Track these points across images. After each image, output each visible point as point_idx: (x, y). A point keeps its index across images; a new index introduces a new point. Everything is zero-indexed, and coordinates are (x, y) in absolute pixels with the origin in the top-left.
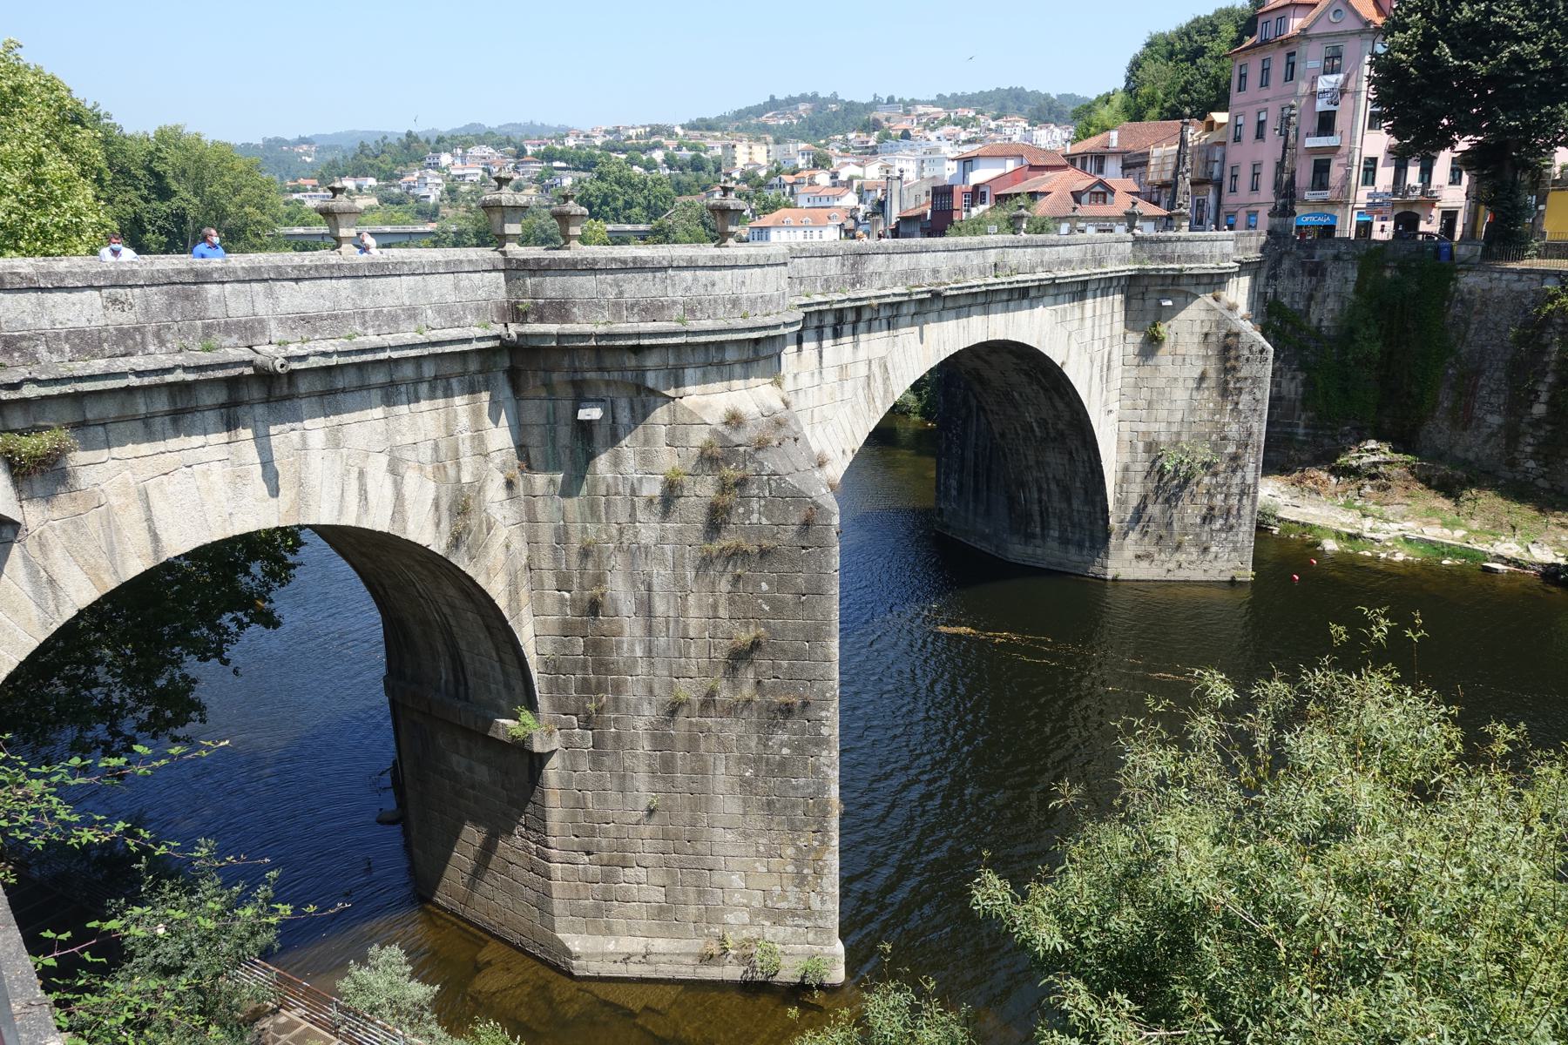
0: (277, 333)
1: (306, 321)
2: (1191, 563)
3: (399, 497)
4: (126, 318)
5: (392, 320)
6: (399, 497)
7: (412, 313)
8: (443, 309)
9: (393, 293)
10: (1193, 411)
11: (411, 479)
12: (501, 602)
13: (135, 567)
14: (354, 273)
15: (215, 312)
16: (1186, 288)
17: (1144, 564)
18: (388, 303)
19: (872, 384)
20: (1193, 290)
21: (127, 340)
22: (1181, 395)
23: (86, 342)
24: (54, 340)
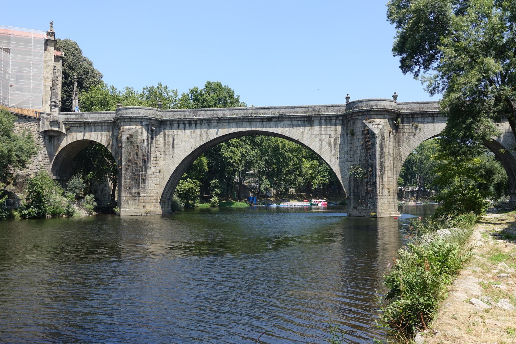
0: (89, 119)
1: (92, 118)
2: (364, 210)
3: (101, 139)
4: (76, 117)
5: (102, 118)
6: (101, 139)
7: (104, 118)
8: (108, 117)
9: (103, 115)
10: (361, 156)
11: (103, 137)
12: (114, 156)
13: (74, 140)
14: (98, 113)
15: (84, 117)
16: (355, 117)
17: (355, 211)
18: (102, 117)
19: (202, 136)
20: (357, 117)
21: (76, 119)
22: (358, 152)
23: (73, 119)
24: (71, 119)
